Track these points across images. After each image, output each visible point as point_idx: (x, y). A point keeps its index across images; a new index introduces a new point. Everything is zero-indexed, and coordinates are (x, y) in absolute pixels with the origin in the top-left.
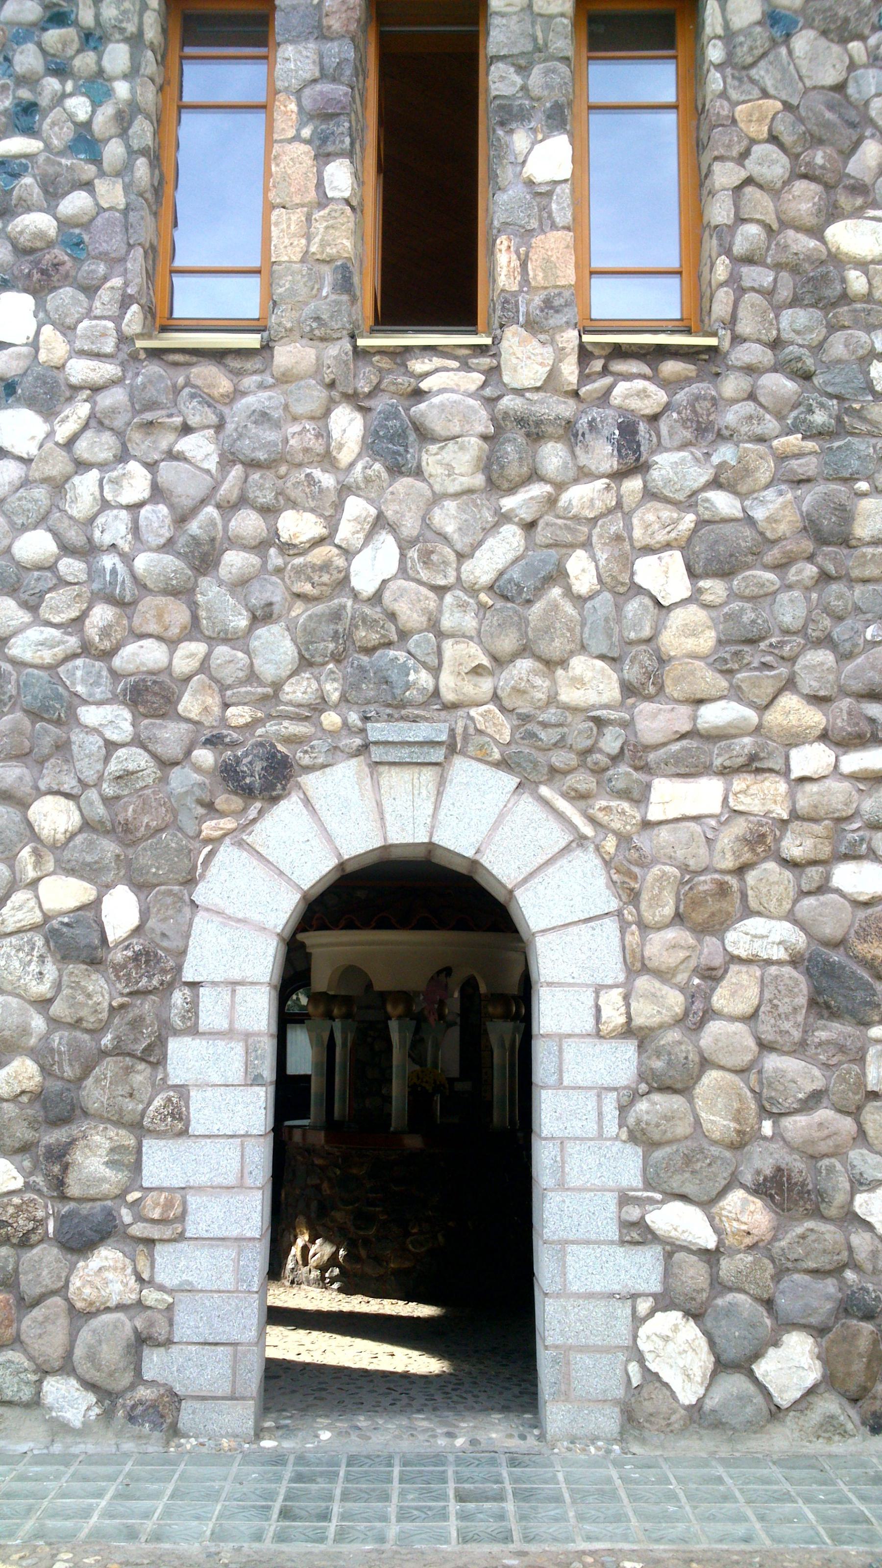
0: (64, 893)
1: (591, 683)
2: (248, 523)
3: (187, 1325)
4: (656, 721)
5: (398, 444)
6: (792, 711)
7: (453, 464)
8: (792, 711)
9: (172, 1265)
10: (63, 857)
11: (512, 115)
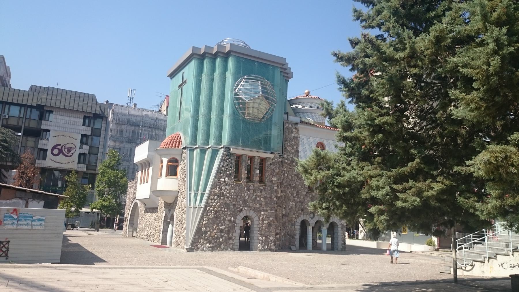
0: (229, 218)
1: (258, 206)
2: (240, 195)
3: (235, 244)
4: (261, 209)
5: (248, 190)
6: (268, 208)
7: (252, 191)
8: (268, 208)
9: (235, 241)
10: (229, 215)
11: (256, 168)
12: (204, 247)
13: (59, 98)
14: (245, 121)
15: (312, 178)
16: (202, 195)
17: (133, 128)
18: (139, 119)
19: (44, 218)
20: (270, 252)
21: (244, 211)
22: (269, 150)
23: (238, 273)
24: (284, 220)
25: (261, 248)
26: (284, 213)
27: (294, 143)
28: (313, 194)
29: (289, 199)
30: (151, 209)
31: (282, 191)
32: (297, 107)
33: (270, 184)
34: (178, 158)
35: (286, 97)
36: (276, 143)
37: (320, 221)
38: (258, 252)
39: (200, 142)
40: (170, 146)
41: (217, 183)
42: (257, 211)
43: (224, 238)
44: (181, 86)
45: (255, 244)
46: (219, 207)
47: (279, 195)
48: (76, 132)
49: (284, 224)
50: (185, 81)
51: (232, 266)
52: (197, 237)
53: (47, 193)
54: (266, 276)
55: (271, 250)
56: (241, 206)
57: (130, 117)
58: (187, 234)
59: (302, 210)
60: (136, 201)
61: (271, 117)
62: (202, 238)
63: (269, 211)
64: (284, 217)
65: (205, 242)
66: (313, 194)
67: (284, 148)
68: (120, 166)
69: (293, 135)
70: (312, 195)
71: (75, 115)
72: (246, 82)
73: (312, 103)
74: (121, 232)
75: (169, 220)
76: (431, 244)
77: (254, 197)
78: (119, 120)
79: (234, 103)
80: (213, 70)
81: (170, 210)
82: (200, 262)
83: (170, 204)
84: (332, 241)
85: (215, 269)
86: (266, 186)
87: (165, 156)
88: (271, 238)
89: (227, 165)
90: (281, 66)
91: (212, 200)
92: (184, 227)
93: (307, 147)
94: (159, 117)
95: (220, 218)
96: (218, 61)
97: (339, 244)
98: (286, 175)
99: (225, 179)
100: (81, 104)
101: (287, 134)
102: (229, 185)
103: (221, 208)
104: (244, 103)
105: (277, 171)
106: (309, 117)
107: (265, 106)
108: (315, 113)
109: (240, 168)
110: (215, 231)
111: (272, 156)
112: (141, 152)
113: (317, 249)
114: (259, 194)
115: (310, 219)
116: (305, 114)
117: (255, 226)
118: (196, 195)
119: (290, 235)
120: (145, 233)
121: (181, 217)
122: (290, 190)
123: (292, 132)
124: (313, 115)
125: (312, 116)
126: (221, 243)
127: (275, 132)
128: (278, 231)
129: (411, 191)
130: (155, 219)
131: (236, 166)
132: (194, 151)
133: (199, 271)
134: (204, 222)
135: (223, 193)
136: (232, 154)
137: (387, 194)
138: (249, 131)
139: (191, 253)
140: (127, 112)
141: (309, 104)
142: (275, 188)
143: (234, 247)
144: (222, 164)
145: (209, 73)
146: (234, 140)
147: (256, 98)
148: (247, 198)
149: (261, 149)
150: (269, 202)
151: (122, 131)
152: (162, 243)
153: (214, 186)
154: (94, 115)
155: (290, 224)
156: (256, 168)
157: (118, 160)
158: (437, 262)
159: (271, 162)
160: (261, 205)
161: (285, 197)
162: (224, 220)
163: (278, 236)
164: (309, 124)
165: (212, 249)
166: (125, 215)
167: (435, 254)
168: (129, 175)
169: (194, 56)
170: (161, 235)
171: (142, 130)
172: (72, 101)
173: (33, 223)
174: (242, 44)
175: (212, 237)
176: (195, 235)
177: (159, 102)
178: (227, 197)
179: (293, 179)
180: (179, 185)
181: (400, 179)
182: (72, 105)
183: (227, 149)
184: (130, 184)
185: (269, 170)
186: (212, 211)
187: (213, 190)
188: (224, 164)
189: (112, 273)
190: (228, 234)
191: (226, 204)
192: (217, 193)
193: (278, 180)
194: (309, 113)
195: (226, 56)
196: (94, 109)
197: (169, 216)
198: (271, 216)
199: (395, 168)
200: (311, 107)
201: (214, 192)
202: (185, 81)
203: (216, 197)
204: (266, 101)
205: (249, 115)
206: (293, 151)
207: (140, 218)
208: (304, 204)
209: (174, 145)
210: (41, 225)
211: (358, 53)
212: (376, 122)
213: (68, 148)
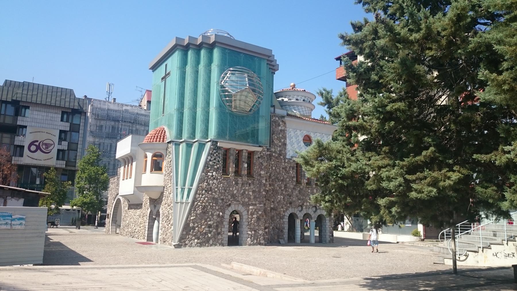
0: (218, 213)
1: (247, 200)
2: (228, 189)
4: (250, 203)
5: (237, 184)
6: (257, 202)
7: (240, 185)
8: (257, 202)
10: (217, 210)
11: (244, 162)
12: (192, 243)
13: (35, 93)
14: (232, 114)
15: (314, 169)
16: (190, 190)
17: (113, 123)
18: (119, 114)
19: (24, 217)
20: (259, 246)
21: (233, 206)
22: (257, 144)
23: (232, 269)
24: (273, 214)
25: (250, 242)
26: (272, 206)
27: (281, 136)
28: (301, 187)
29: (277, 193)
30: (135, 206)
31: (270, 184)
32: (283, 100)
33: (259, 178)
34: (164, 153)
35: (272, 89)
36: (263, 137)
37: (308, 214)
38: (247, 246)
39: (185, 136)
40: (155, 140)
41: (204, 178)
42: (246, 205)
43: (212, 233)
44: (164, 78)
45: (244, 239)
46: (207, 201)
47: (267, 189)
48: (54, 127)
49: (272, 218)
50: (169, 74)
51: (224, 262)
52: (184, 233)
53: (27, 190)
54: (262, 272)
55: (260, 244)
56: (229, 201)
57: (109, 112)
58: (174, 230)
59: (291, 203)
60: (118, 197)
61: (259, 110)
62: (189, 234)
63: (258, 205)
64: (272, 211)
65: (194, 238)
66: (301, 187)
67: (271, 142)
68: (100, 162)
69: (280, 128)
70: (300, 188)
71: (52, 111)
72: (232, 74)
73: (298, 96)
74: (104, 229)
75: (154, 216)
76: (416, 234)
77: (242, 191)
78: (98, 115)
79: (221, 96)
80: (198, 62)
81: (155, 206)
82: (190, 258)
83: (156, 200)
84: (320, 233)
85: (208, 266)
86: (254, 180)
87: (149, 150)
88: (260, 232)
89: (215, 159)
90: (267, 58)
91: (199, 194)
92: (171, 223)
93: (294, 140)
94: (139, 112)
95: (208, 213)
96: (203, 52)
97: (327, 237)
98: (274, 168)
99: (212, 173)
100: (58, 99)
101: (274, 127)
102: (217, 179)
103: (209, 203)
104: (230, 96)
105: (265, 164)
106: (295, 110)
107: (252, 99)
108: (301, 106)
109: (228, 162)
110: (203, 227)
111: (260, 149)
112: (124, 147)
113: (305, 242)
114: (247, 188)
115: (298, 212)
116: (292, 107)
117: (244, 220)
118: (183, 190)
119: (279, 229)
120: (130, 230)
121: (167, 213)
122: (278, 183)
123: (279, 125)
124: (300, 107)
125: (299, 109)
126: (209, 239)
127: (262, 125)
128: (267, 225)
129: (426, 181)
130: (140, 216)
131: (224, 160)
132: (179, 145)
133: (192, 269)
134: (192, 218)
135: (211, 188)
136: (220, 148)
137: (400, 185)
138: (236, 124)
139: (179, 249)
140: (106, 107)
141: (295, 97)
142: (264, 181)
143: (222, 242)
144: (209, 158)
145: (194, 65)
146: (221, 133)
147: (243, 91)
148: (235, 192)
149: (248, 142)
150: (257, 196)
151: (102, 126)
152: (148, 240)
153: (201, 181)
154: (72, 111)
155: (279, 217)
156: (244, 162)
157: (98, 156)
158: (426, 252)
159: (259, 156)
160: (249, 199)
161: (273, 190)
162: (212, 215)
163: (267, 230)
164: (295, 117)
165: (201, 245)
166: (108, 212)
167: (421, 244)
168: (110, 171)
169: (178, 47)
170: (146, 232)
171: (122, 125)
172: (49, 96)
173: (13, 222)
174: (226, 35)
175: (201, 232)
176: (183, 231)
177: (139, 97)
178: (215, 192)
179: (281, 172)
180: (165, 180)
181: (412, 169)
182: (49, 100)
183: (214, 143)
184: (112, 180)
185: (257, 164)
186: (199, 206)
187: (201, 185)
188: (211, 157)
189: (101, 274)
190: (217, 229)
191: (214, 198)
192: (204, 188)
193: (267, 174)
194: (295, 106)
195: (211, 47)
196: (72, 104)
197: (155, 212)
198: (259, 210)
199: (408, 158)
200: (297, 100)
201: (201, 187)
202: (169, 74)
203: (204, 191)
204: (253, 93)
205: (236, 108)
206: (280, 144)
207: (123, 214)
208: (292, 198)
209: (158, 140)
210: (21, 224)
211: (366, 36)
212: (388, 108)
213: (46, 144)
